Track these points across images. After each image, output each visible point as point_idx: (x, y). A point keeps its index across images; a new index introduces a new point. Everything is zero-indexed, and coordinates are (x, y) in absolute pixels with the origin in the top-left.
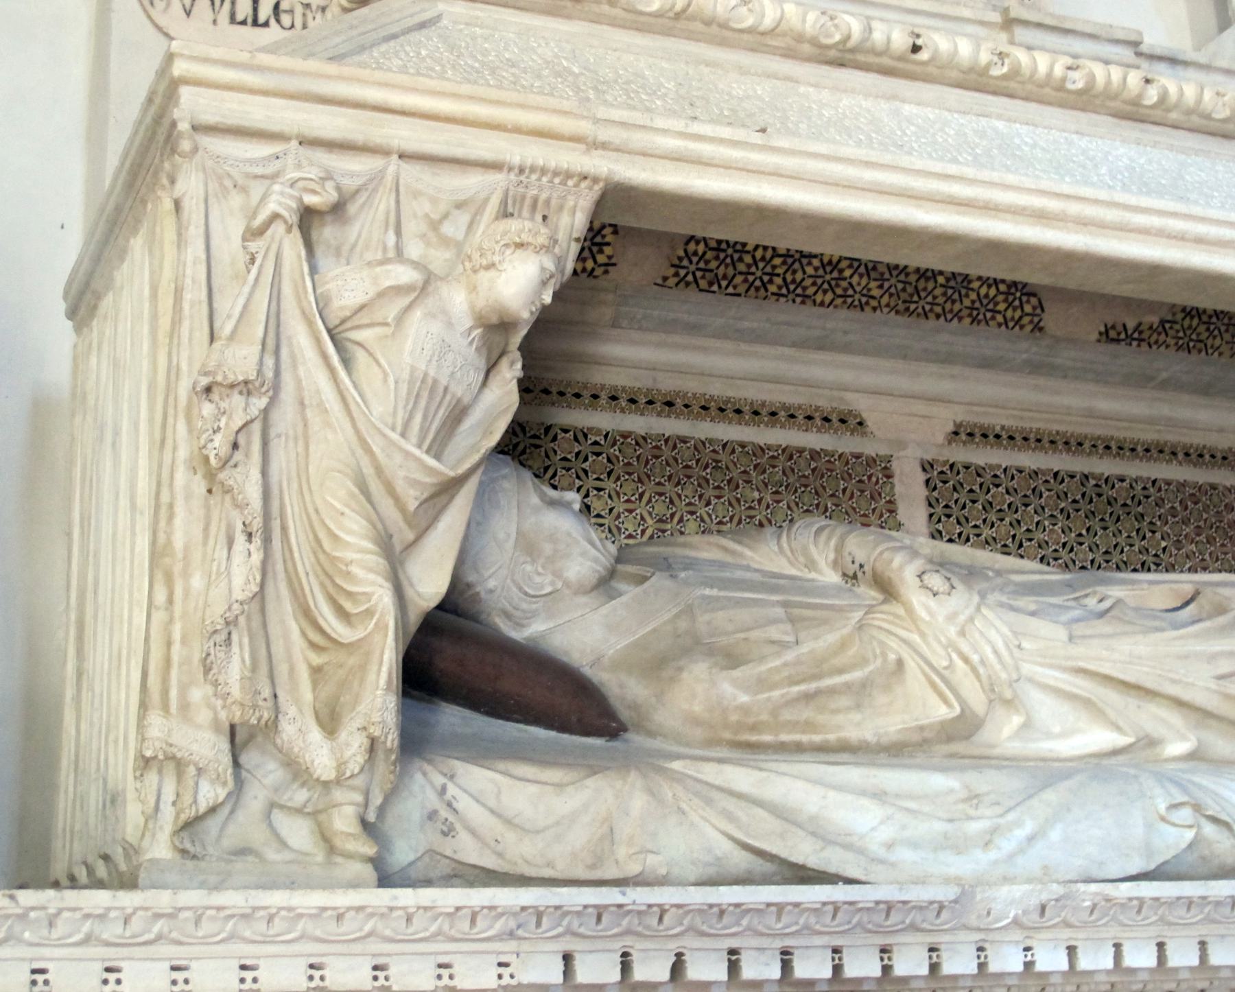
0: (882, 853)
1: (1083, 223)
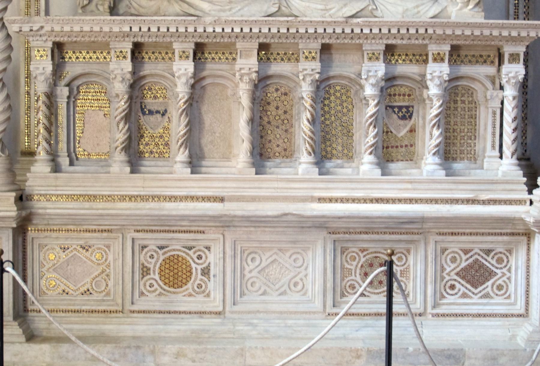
0: (208, 12)
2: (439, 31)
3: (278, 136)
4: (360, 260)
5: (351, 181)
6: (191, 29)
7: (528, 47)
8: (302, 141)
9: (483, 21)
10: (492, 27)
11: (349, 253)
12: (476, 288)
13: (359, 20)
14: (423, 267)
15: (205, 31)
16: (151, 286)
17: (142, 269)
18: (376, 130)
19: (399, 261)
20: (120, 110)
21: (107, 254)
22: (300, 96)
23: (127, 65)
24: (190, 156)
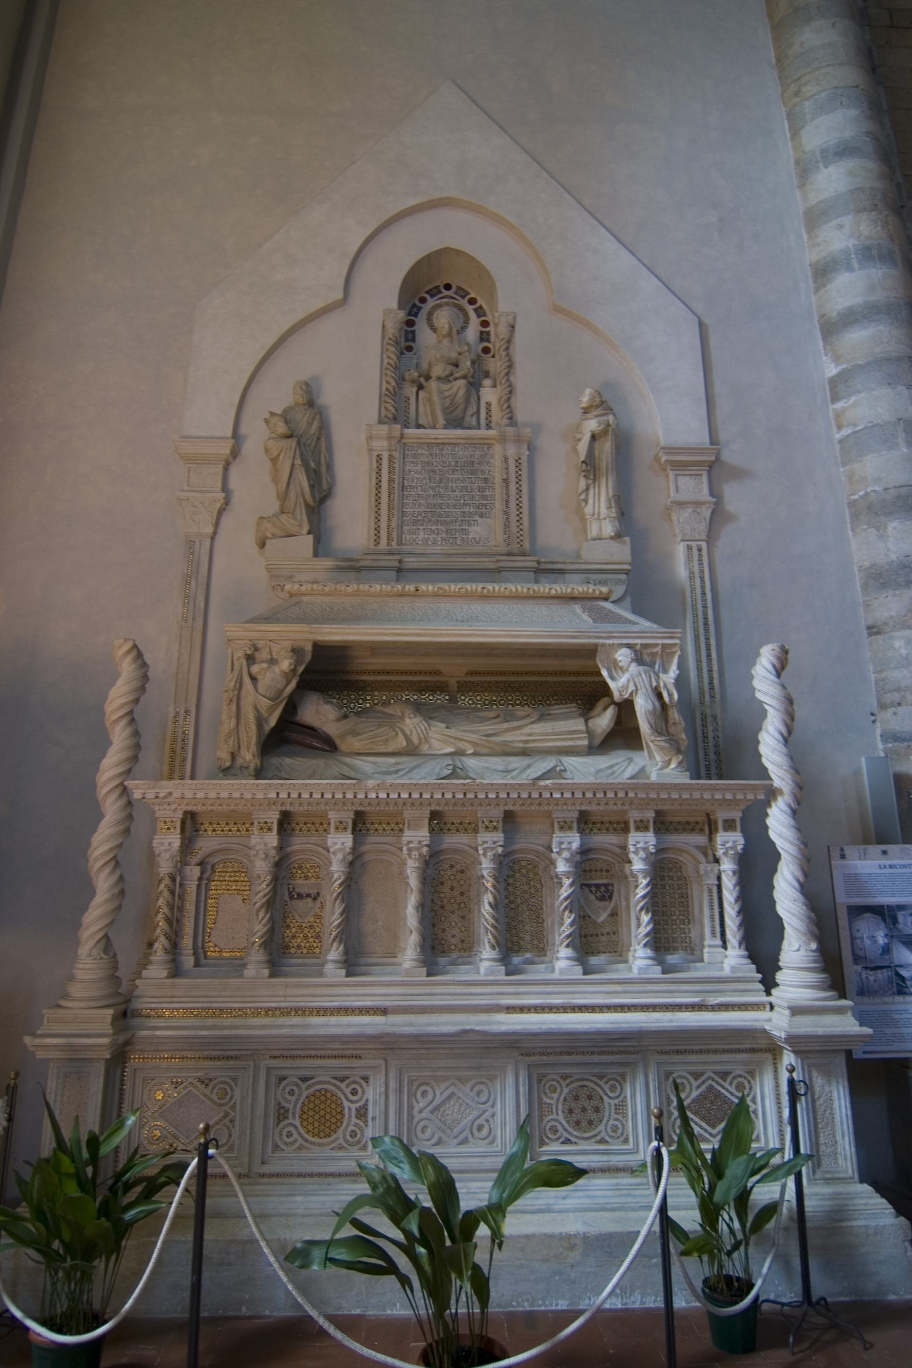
1: (431, 635)
2: (642, 795)
3: (454, 924)
4: (562, 1091)
5: (546, 983)
6: (350, 795)
7: (743, 812)
8: (482, 931)
9: (689, 781)
10: (703, 788)
11: (548, 1081)
12: (714, 1127)
13: (548, 782)
14: (644, 1099)
15: (366, 797)
16: (289, 1135)
17: (278, 1111)
18: (573, 916)
19: (612, 1091)
20: (261, 894)
21: (232, 1089)
22: (479, 874)
23: (272, 840)
24: (346, 952)
